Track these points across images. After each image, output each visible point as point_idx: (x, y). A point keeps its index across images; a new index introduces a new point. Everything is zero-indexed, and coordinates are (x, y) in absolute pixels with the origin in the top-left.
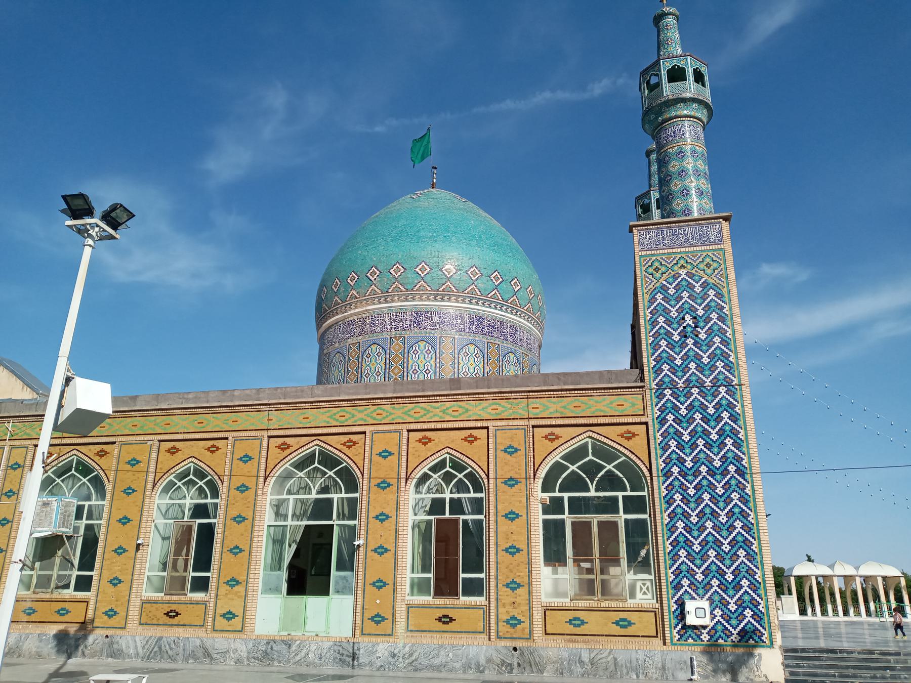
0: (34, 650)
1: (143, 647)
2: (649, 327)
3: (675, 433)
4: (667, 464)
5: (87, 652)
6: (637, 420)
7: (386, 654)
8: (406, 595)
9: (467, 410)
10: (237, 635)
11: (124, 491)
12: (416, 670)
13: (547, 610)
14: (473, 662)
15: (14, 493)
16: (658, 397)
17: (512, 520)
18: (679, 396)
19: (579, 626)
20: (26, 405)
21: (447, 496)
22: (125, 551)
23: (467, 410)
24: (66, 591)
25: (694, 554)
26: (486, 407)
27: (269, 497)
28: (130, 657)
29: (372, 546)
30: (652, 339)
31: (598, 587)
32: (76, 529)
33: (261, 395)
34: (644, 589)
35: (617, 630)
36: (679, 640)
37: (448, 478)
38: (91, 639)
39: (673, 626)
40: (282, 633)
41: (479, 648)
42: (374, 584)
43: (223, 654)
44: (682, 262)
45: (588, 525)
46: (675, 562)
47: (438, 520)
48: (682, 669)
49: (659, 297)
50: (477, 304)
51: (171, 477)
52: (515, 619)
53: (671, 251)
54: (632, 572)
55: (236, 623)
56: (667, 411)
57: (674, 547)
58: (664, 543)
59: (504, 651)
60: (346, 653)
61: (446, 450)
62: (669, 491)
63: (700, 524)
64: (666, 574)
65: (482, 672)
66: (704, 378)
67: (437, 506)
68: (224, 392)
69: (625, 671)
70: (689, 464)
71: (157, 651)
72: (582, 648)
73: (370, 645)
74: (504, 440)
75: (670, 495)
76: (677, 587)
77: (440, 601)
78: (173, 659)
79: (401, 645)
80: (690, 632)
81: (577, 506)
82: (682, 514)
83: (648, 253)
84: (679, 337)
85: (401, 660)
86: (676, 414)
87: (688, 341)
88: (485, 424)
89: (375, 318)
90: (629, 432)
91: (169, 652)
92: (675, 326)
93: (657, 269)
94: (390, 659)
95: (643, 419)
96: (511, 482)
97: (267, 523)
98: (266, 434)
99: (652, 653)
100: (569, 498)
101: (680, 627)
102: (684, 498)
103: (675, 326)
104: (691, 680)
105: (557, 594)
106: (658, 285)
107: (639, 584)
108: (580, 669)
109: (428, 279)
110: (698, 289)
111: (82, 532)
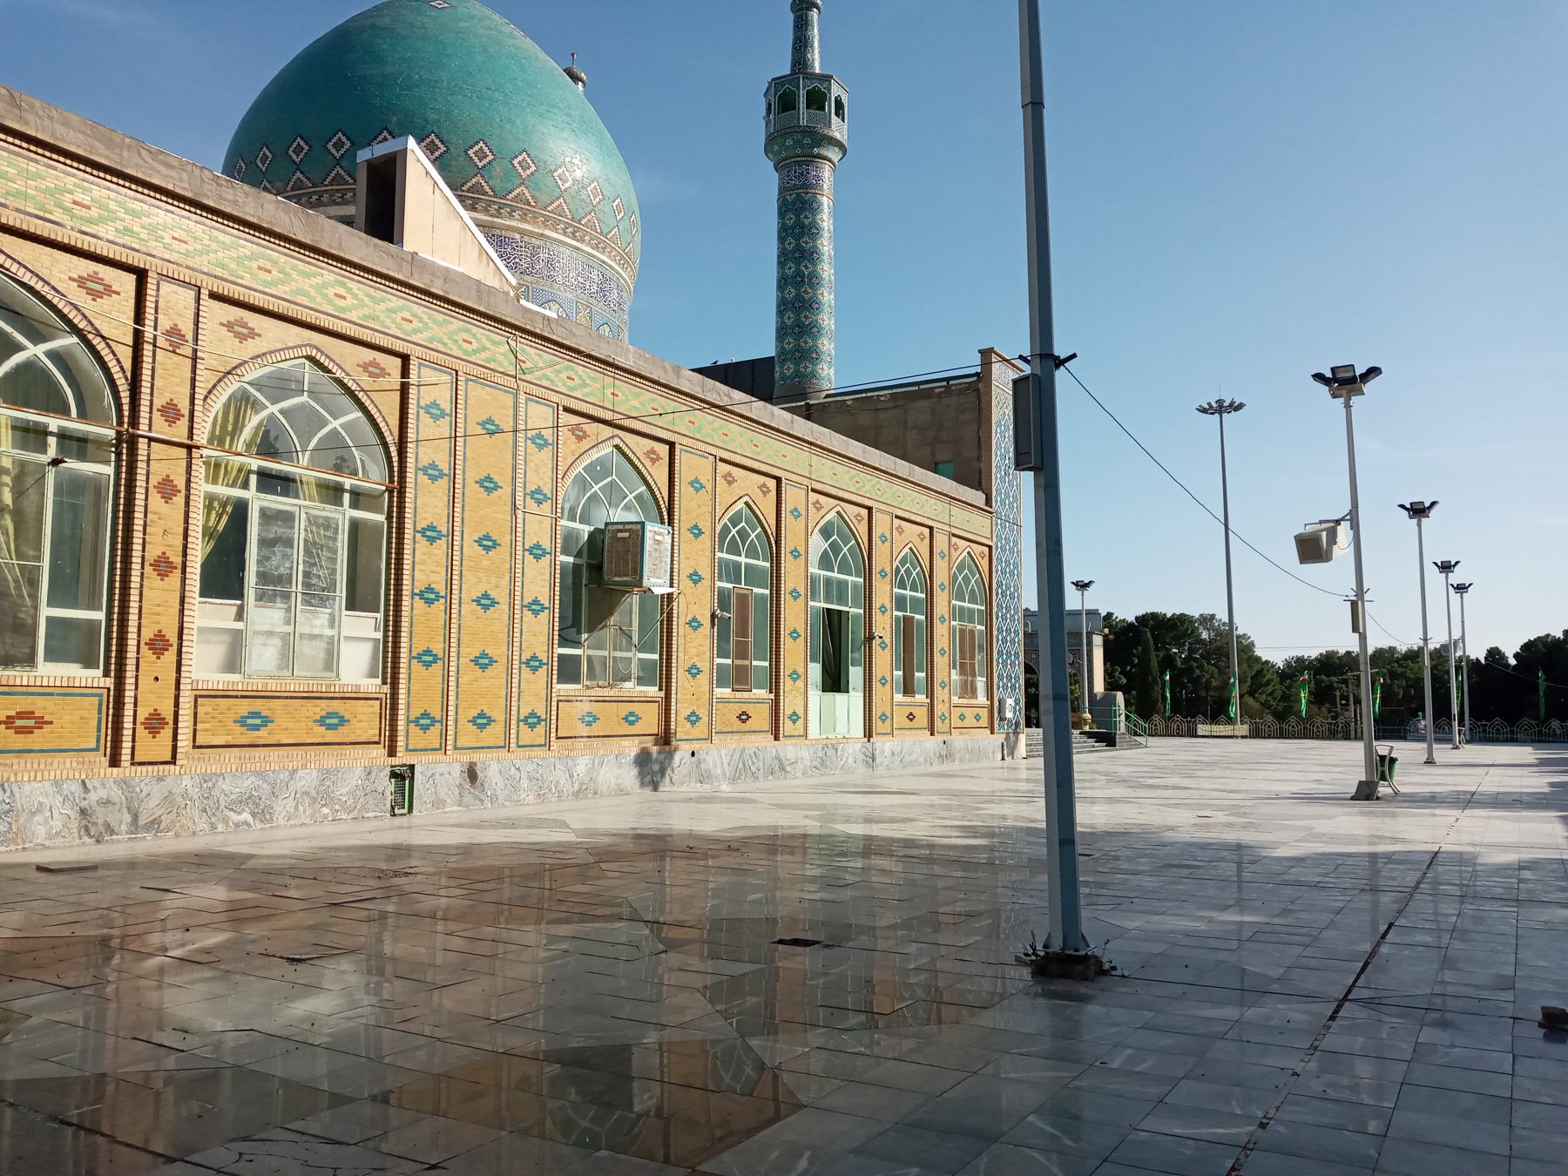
0: (614, 781)
24: (628, 685)
38: (677, 757)
41: (932, 743)
77: (908, 699)
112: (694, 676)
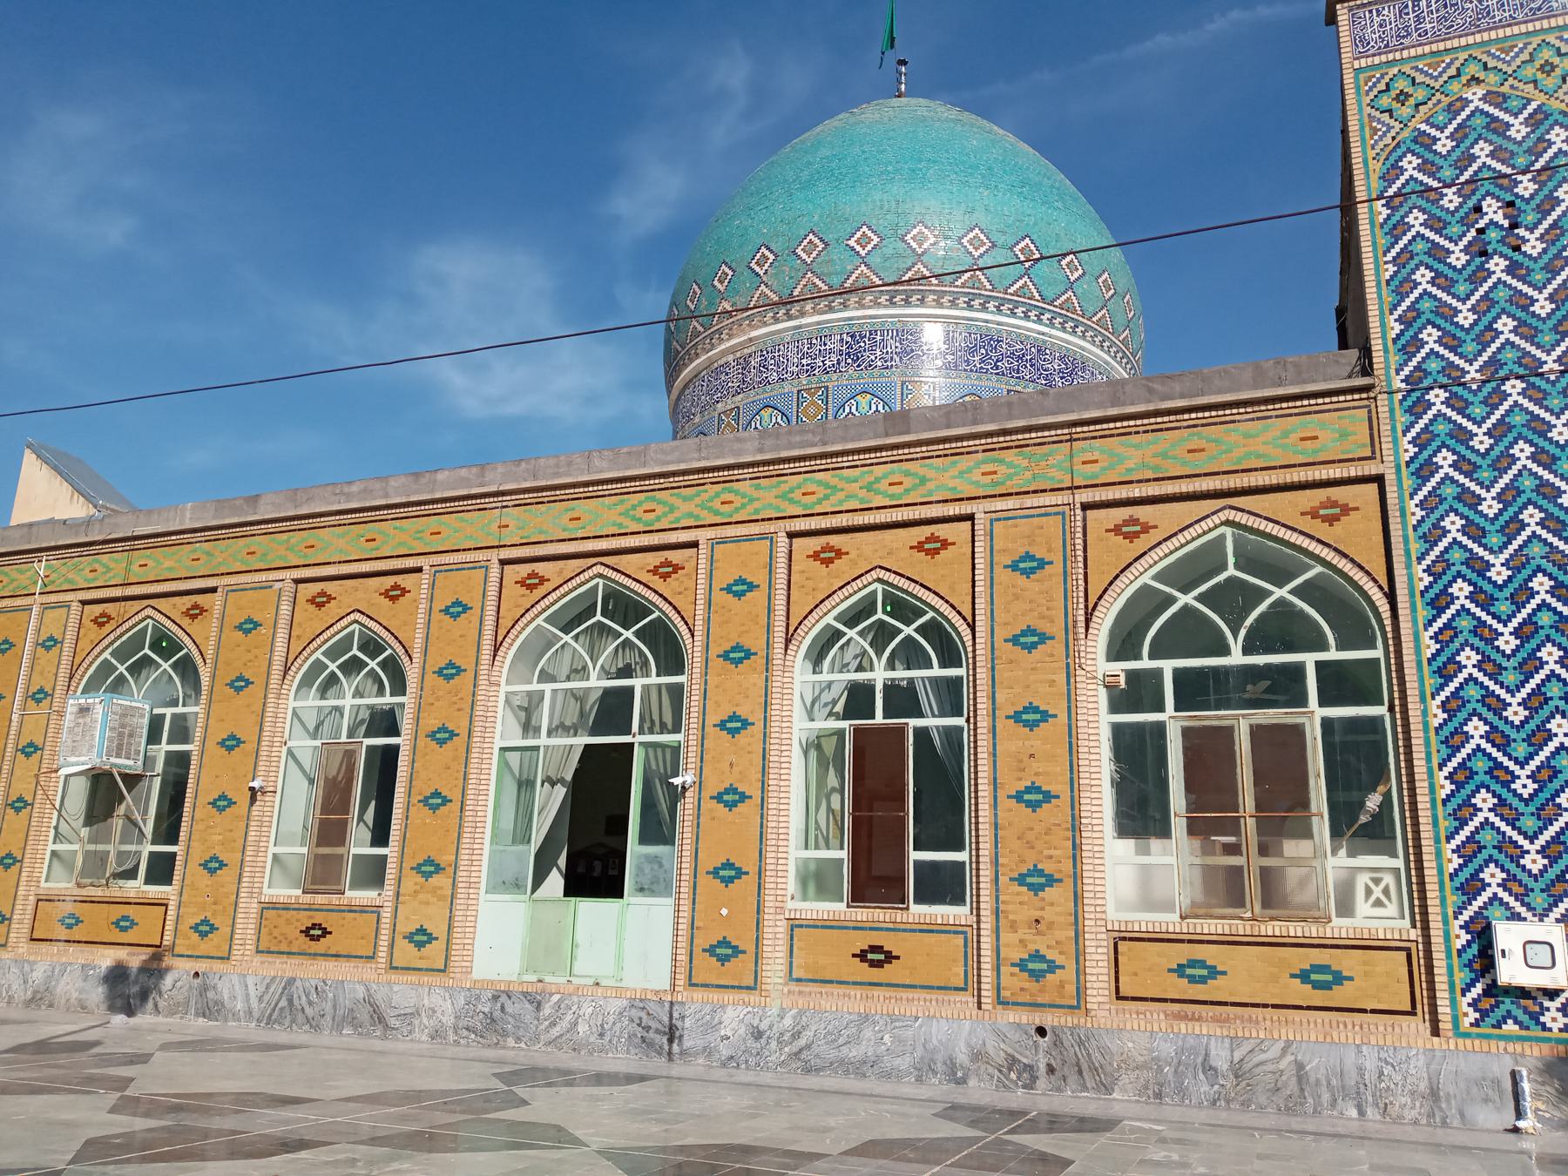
0: (75, 995)
1: (260, 999)
2: (1383, 241)
3: (1458, 498)
4: (1437, 577)
5: (162, 1004)
6: (1353, 471)
7: (742, 1031)
8: (788, 897)
9: (923, 481)
10: (435, 979)
11: (231, 684)
12: (808, 1070)
13: (1122, 939)
14: (940, 1057)
15: (47, 694)
16: (1409, 411)
17: (1032, 725)
18: (1468, 404)
19: (1202, 980)
20: (71, 526)
21: (879, 675)
22: (231, 803)
23: (923, 481)
24: (131, 883)
25: (1515, 803)
26: (969, 471)
27: (504, 688)
28: (235, 1016)
29: (713, 786)
30: (1392, 269)
31: (1252, 886)
32: (148, 761)
33: (489, 476)
34: (1378, 892)
35: (1302, 993)
36: (1476, 1024)
37: (881, 635)
38: (168, 981)
39: (1459, 986)
40: (526, 978)
41: (954, 1026)
42: (715, 873)
43: (409, 1017)
44: (1473, 69)
45: (1226, 734)
46: (1463, 823)
47: (858, 731)
48: (1486, 1100)
49: (1410, 164)
50: (984, 308)
51: (318, 655)
52: (1042, 958)
53: (1441, 46)
54: (1343, 852)
55: (435, 950)
56: (1435, 445)
57: (1460, 786)
58: (1431, 774)
59: (1015, 1036)
60: (654, 1025)
61: (874, 574)
62: (1444, 645)
63: (1532, 725)
64: (1439, 854)
65: (962, 1082)
66: (1539, 354)
67: (858, 699)
68: (417, 475)
69: (1326, 1097)
70: (1499, 573)
71: (285, 1008)
72: (1215, 1039)
73: (708, 1009)
74: (1012, 541)
75: (1447, 653)
76: (1472, 887)
77: (862, 914)
78: (314, 1025)
79: (775, 1011)
80: (1507, 1004)
81: (1193, 690)
82: (1482, 701)
83: (1377, 60)
84: (1464, 258)
85: (774, 1044)
86: (1462, 449)
87: (1491, 265)
88: (965, 508)
89: (769, 353)
90: (1334, 504)
91: (308, 1011)
92: (1455, 230)
93: (1402, 97)
94: (750, 1043)
95: (1371, 469)
96: (1030, 639)
97: (499, 743)
98: (495, 556)
99: (1402, 1055)
100: (1179, 674)
101: (1478, 989)
102: (1485, 659)
103: (1455, 230)
104: (1516, 1130)
105: (1148, 902)
106: (1406, 134)
107: (1363, 880)
108: (1205, 1088)
109: (875, 260)
110: (1518, 130)
111: (159, 767)
112: (212, 871)
